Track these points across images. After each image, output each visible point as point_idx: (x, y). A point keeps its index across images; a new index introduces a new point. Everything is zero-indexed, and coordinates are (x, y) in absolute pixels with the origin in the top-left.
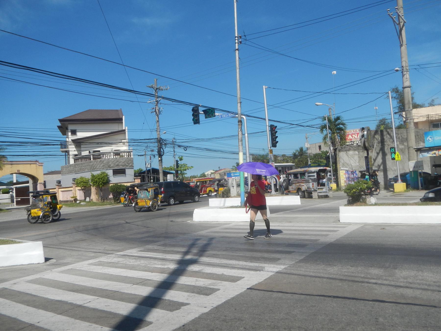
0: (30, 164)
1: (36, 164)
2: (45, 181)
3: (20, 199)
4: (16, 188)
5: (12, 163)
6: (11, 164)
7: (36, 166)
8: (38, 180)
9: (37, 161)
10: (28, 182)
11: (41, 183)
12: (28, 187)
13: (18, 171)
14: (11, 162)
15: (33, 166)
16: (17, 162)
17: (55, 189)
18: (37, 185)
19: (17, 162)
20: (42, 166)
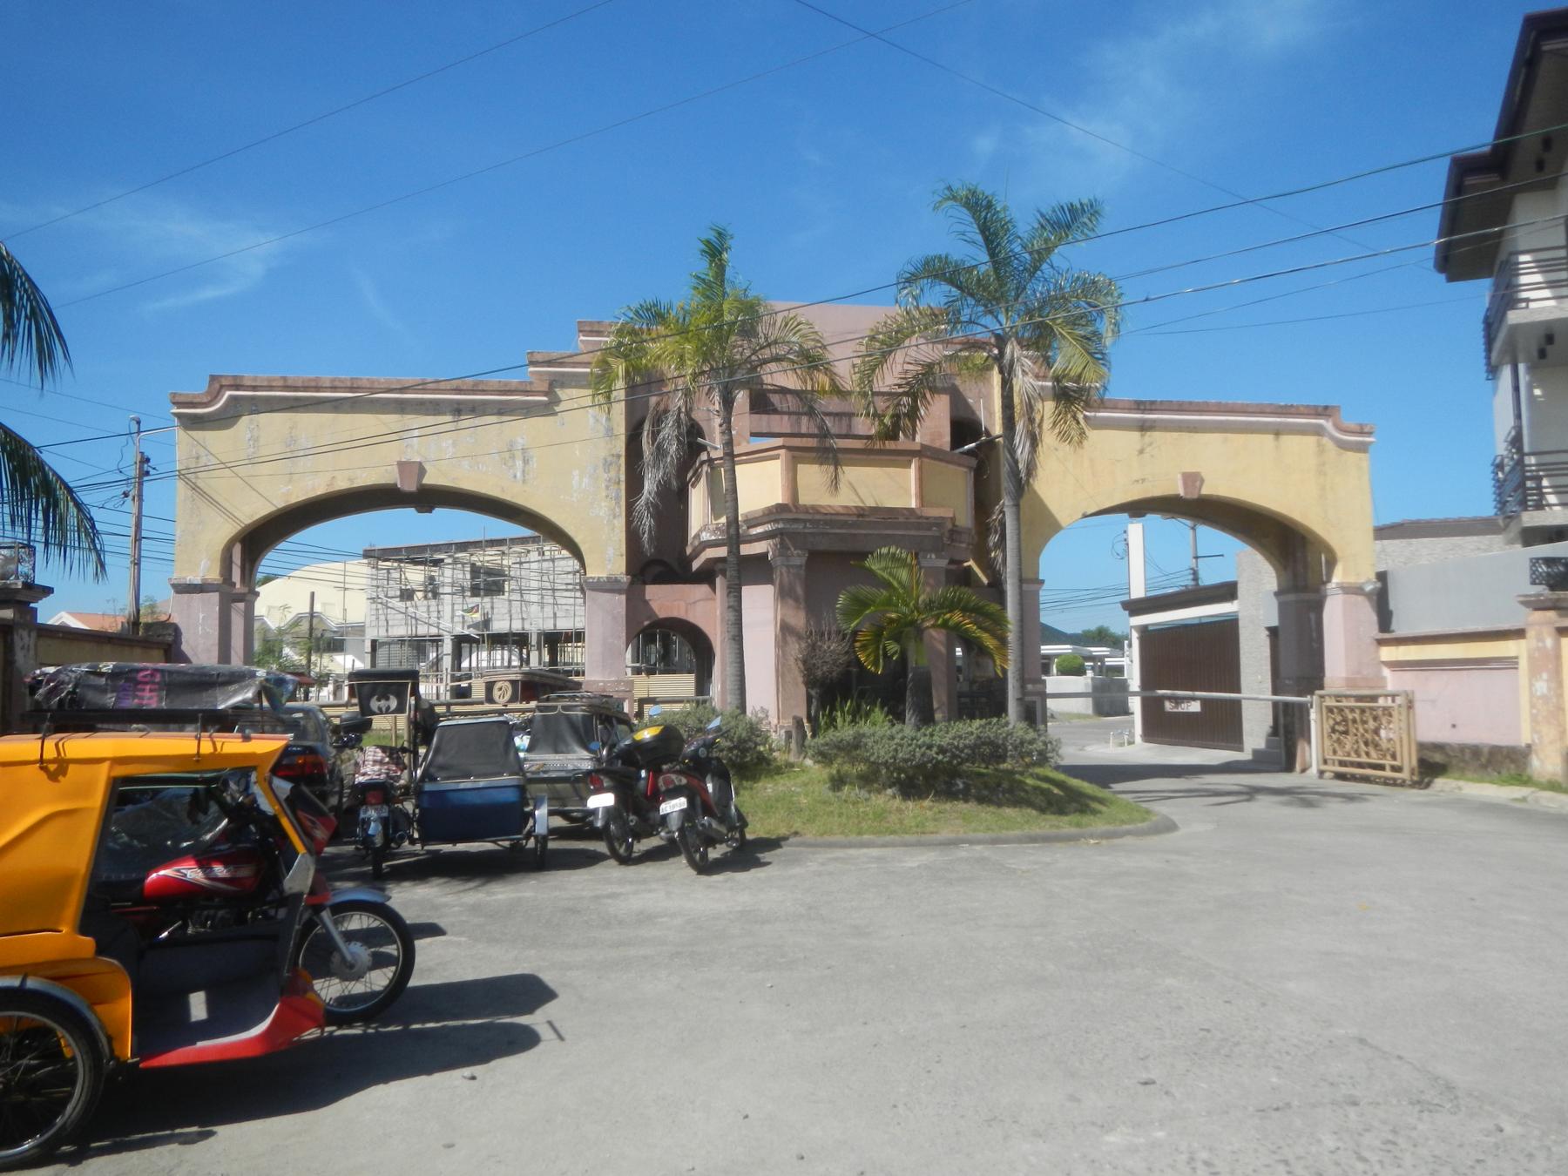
0: (1278, 432)
1: (1318, 431)
2: (1382, 577)
3: (1195, 707)
4: (1144, 631)
5: (1147, 415)
6: (1144, 427)
7: (1321, 450)
8: (1332, 563)
9: (1325, 411)
10: (1227, 592)
11: (1357, 590)
12: (1227, 631)
13: (1192, 479)
14: (1140, 406)
15: (1299, 447)
16: (1181, 408)
17: (1519, 634)
18: (1318, 606)
19: (1181, 408)
20: (1362, 448)
